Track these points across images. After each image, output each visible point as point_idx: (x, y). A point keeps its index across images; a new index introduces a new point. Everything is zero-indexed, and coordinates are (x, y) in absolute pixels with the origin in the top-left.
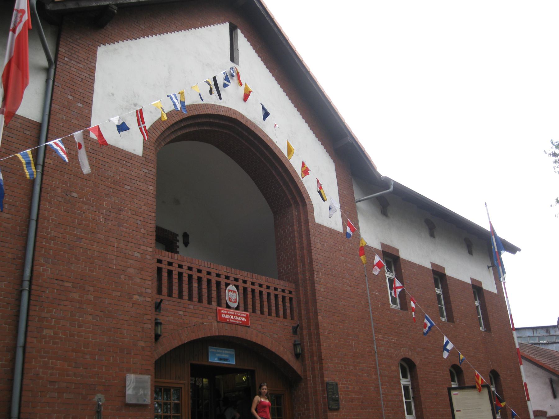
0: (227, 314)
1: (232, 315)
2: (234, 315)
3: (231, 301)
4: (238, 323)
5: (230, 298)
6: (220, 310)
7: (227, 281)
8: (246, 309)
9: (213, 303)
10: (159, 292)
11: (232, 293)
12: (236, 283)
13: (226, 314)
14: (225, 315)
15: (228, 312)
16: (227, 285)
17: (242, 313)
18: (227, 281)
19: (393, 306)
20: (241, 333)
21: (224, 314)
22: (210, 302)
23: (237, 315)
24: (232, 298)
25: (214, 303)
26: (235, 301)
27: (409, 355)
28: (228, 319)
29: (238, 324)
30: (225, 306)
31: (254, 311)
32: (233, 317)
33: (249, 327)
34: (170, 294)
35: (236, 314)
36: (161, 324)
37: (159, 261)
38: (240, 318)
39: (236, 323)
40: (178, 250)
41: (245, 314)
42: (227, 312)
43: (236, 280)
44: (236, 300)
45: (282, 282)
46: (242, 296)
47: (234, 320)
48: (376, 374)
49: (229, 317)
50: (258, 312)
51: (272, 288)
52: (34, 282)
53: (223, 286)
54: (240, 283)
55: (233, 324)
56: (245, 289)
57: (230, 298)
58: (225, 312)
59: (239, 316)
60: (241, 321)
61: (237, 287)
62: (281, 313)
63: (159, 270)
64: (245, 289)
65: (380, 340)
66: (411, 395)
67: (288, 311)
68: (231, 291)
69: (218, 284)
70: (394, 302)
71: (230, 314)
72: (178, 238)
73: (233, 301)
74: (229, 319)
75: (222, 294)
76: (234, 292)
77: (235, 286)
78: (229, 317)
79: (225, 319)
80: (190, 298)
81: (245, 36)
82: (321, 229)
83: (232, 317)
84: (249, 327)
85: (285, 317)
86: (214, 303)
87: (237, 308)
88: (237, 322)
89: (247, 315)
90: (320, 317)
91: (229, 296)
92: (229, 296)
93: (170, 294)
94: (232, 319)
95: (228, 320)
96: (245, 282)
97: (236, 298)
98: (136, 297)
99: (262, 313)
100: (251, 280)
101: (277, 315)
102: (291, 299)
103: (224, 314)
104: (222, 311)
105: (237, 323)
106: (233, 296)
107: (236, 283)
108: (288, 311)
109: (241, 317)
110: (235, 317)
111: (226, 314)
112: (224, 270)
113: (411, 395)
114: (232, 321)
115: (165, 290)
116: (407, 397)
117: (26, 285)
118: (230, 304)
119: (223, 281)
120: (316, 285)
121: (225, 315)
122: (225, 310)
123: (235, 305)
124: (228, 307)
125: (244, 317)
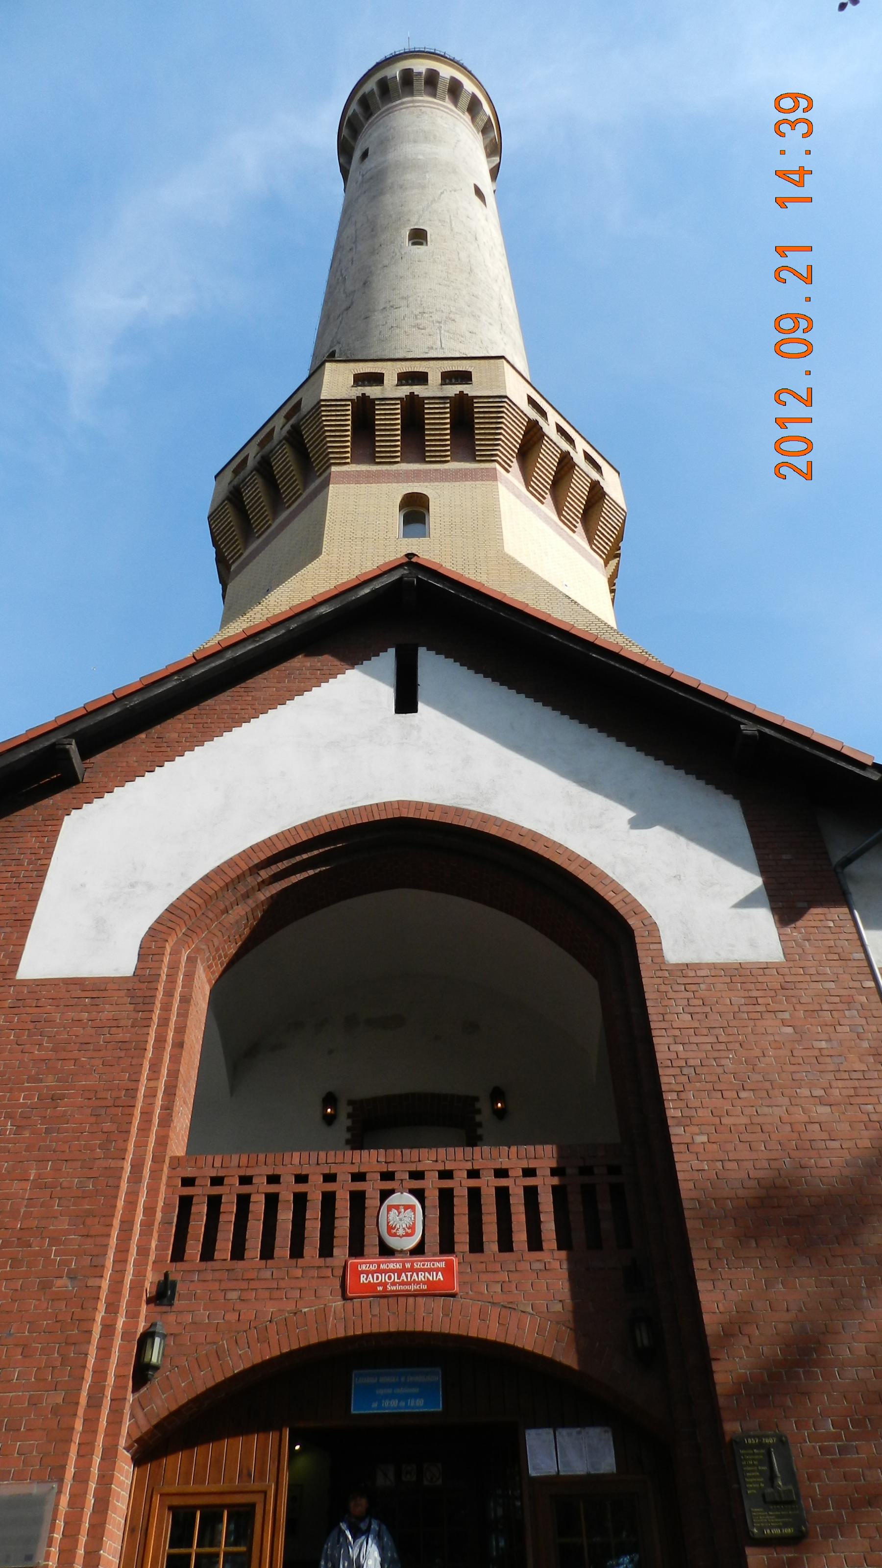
1: (393, 1271)
2: (399, 1272)
3: (395, 1235)
4: (415, 1291)
6: (355, 1266)
8: (447, 1246)
10: (178, 1254)
11: (399, 1213)
12: (417, 1184)
14: (370, 1276)
15: (382, 1267)
16: (385, 1195)
17: (431, 1261)
21: (367, 1273)
22: (326, 1250)
23: (412, 1270)
24: (398, 1226)
26: (409, 1231)
28: (380, 1284)
29: (416, 1295)
30: (377, 1250)
32: (399, 1278)
33: (453, 1296)
35: (408, 1266)
37: (188, 1182)
39: (407, 1291)
40: (480, 1131)
41: (439, 1261)
42: (379, 1266)
43: (417, 1175)
44: (412, 1228)
46: (435, 1214)
47: (403, 1283)
49: (383, 1278)
53: (372, 1200)
55: (398, 1296)
56: (446, 1197)
57: (390, 1228)
58: (373, 1267)
59: (418, 1271)
60: (428, 1282)
61: (419, 1194)
63: (186, 1203)
64: (446, 1197)
68: (397, 1207)
69: (358, 1200)
71: (385, 1272)
72: (478, 1105)
73: (401, 1232)
74: (384, 1285)
76: (413, 1208)
77: (412, 1192)
78: (383, 1278)
79: (372, 1286)
82: (692, 974)
83: (395, 1277)
84: (453, 1296)
86: (341, 1251)
87: (419, 1250)
88: (413, 1287)
89: (449, 1265)
91: (388, 1223)
92: (388, 1223)
94: (394, 1284)
95: (380, 1288)
97: (414, 1224)
99: (506, 1244)
103: (367, 1273)
105: (410, 1291)
106: (401, 1220)
107: (417, 1184)
110: (403, 1274)
111: (373, 1272)
114: (394, 1288)
115: (194, 1248)
118: (393, 1242)
121: (370, 1276)
122: (372, 1263)
123: (412, 1242)
124: (386, 1251)
125: (437, 1270)
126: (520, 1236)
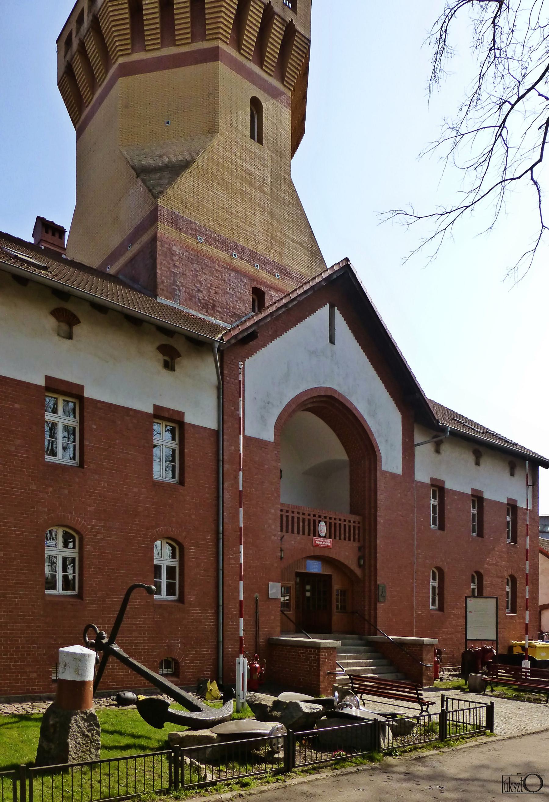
0: (319, 541)
5: (321, 531)
7: (320, 519)
8: (330, 537)
9: (311, 535)
12: (325, 520)
13: (319, 541)
16: (320, 521)
18: (320, 519)
19: (433, 527)
20: (326, 553)
22: (309, 535)
25: (312, 534)
27: (440, 564)
31: (335, 538)
34: (287, 531)
36: (283, 551)
38: (326, 544)
43: (325, 517)
45: (354, 516)
46: (328, 528)
48: (413, 579)
50: (338, 538)
51: (347, 521)
52: (224, 534)
54: (327, 520)
56: (330, 523)
57: (321, 531)
62: (352, 538)
63: (282, 516)
64: (330, 523)
65: (419, 554)
66: (437, 592)
67: (357, 536)
69: (314, 521)
70: (434, 523)
71: (320, 541)
75: (317, 528)
79: (318, 545)
80: (298, 533)
81: (340, 313)
85: (354, 540)
86: (312, 534)
87: (325, 537)
90: (378, 541)
93: (287, 531)
96: (330, 518)
98: (273, 537)
99: (340, 539)
100: (334, 517)
101: (349, 540)
102: (359, 527)
104: (316, 540)
108: (357, 536)
109: (328, 542)
112: (317, 512)
113: (437, 592)
115: (284, 529)
116: (434, 593)
117: (221, 535)
119: (317, 519)
120: (378, 518)
124: (320, 536)
126: (343, 537)
